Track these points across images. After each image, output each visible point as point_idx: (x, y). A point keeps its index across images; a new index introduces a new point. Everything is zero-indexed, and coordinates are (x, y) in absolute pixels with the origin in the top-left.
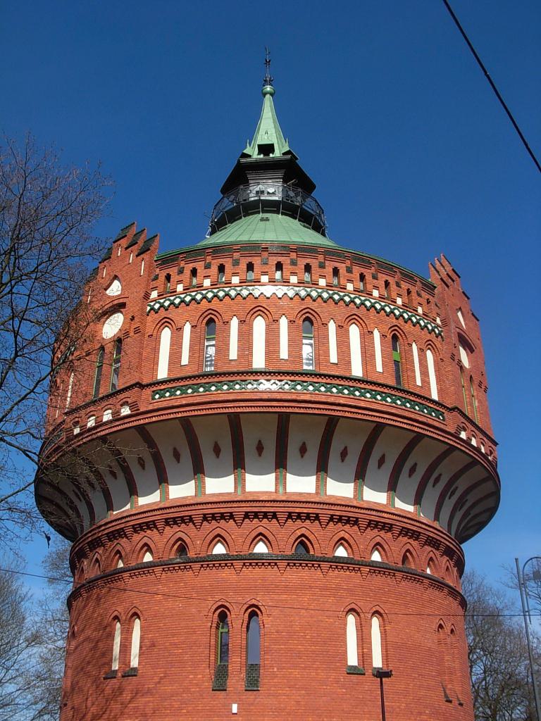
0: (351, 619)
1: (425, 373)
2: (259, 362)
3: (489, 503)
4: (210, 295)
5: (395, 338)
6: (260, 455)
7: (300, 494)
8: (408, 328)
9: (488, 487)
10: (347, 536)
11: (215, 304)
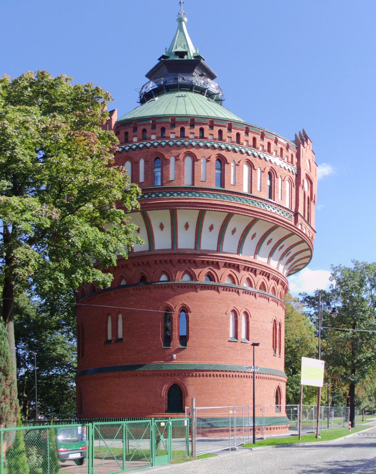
3: (307, 260)
6: (187, 229)
9: (308, 253)
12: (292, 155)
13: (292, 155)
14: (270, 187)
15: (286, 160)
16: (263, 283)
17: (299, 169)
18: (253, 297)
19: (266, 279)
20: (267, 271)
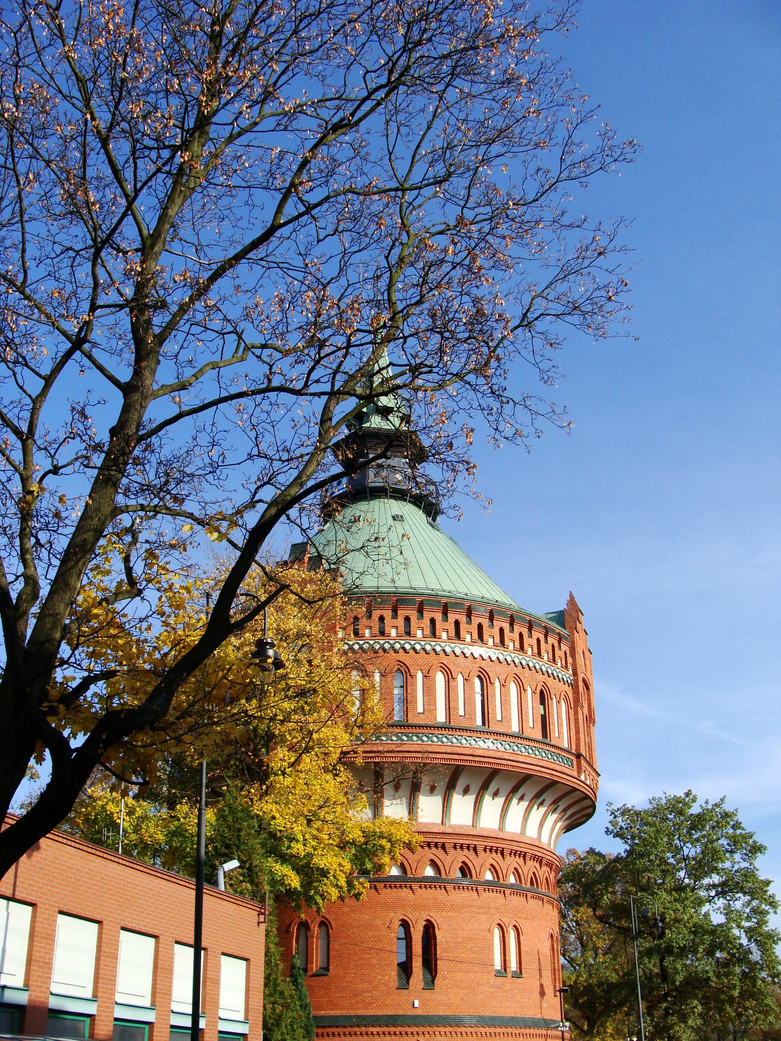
0: (497, 932)
1: (560, 725)
2: (441, 717)
4: (397, 646)
5: (541, 691)
7: (461, 827)
8: (550, 682)
10: (495, 864)
11: (402, 656)
12: (565, 653)
13: (565, 653)
14: (544, 718)
15: (559, 664)
16: (534, 873)
17: (575, 674)
18: (523, 899)
19: (538, 865)
20: (540, 854)
